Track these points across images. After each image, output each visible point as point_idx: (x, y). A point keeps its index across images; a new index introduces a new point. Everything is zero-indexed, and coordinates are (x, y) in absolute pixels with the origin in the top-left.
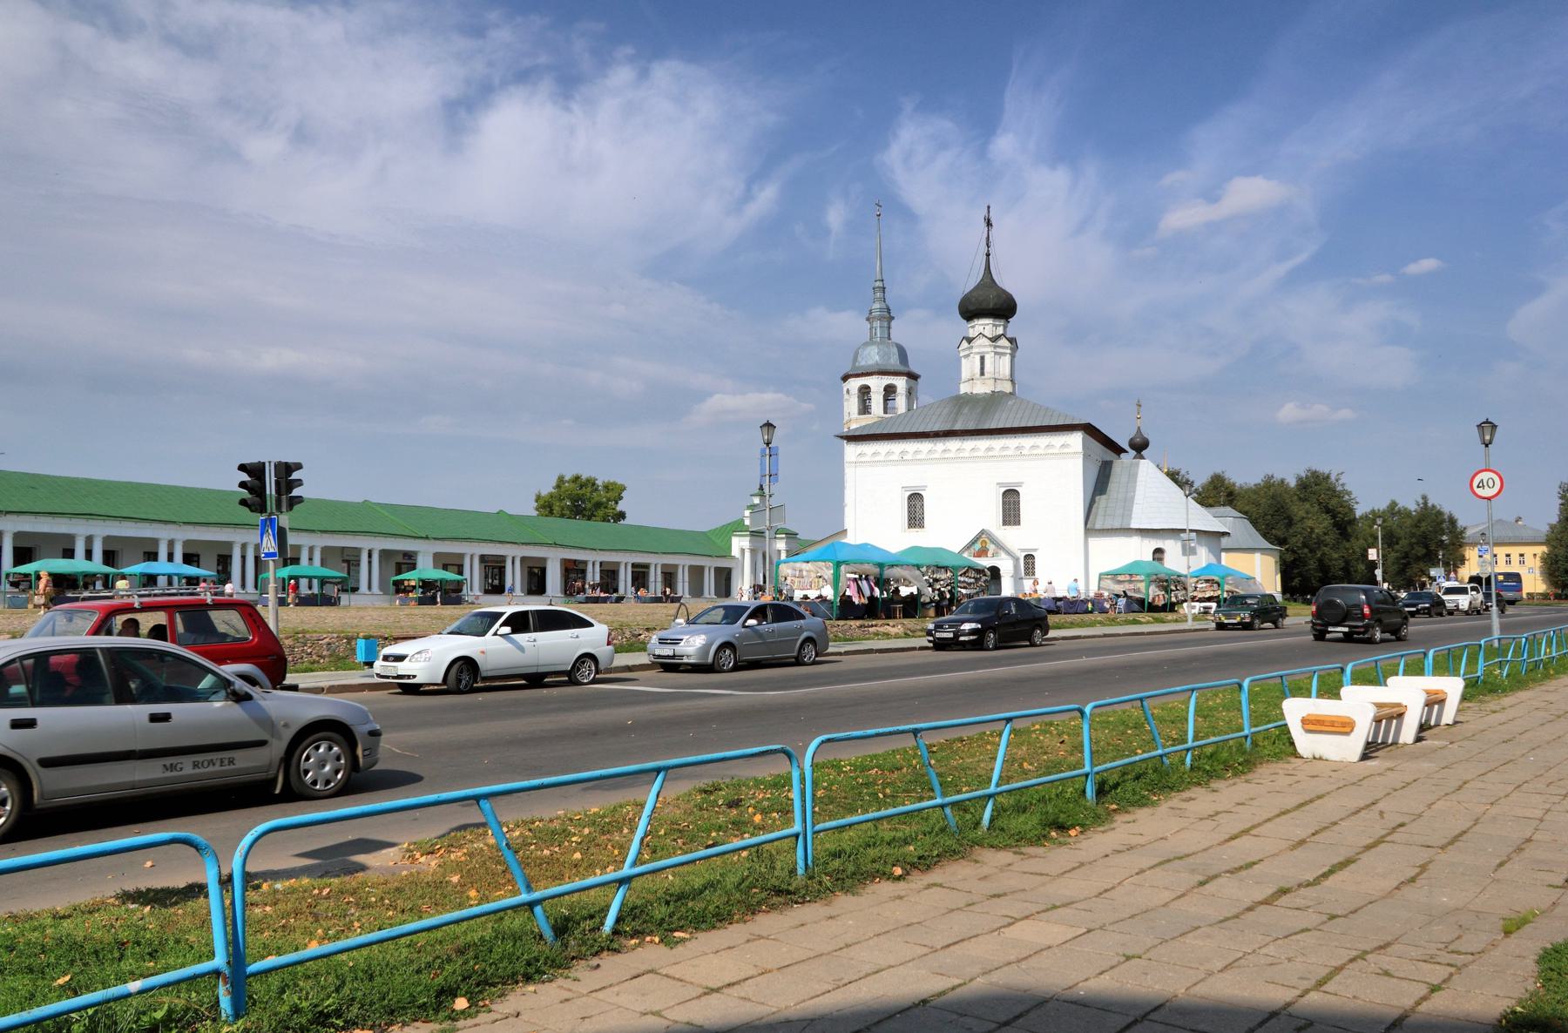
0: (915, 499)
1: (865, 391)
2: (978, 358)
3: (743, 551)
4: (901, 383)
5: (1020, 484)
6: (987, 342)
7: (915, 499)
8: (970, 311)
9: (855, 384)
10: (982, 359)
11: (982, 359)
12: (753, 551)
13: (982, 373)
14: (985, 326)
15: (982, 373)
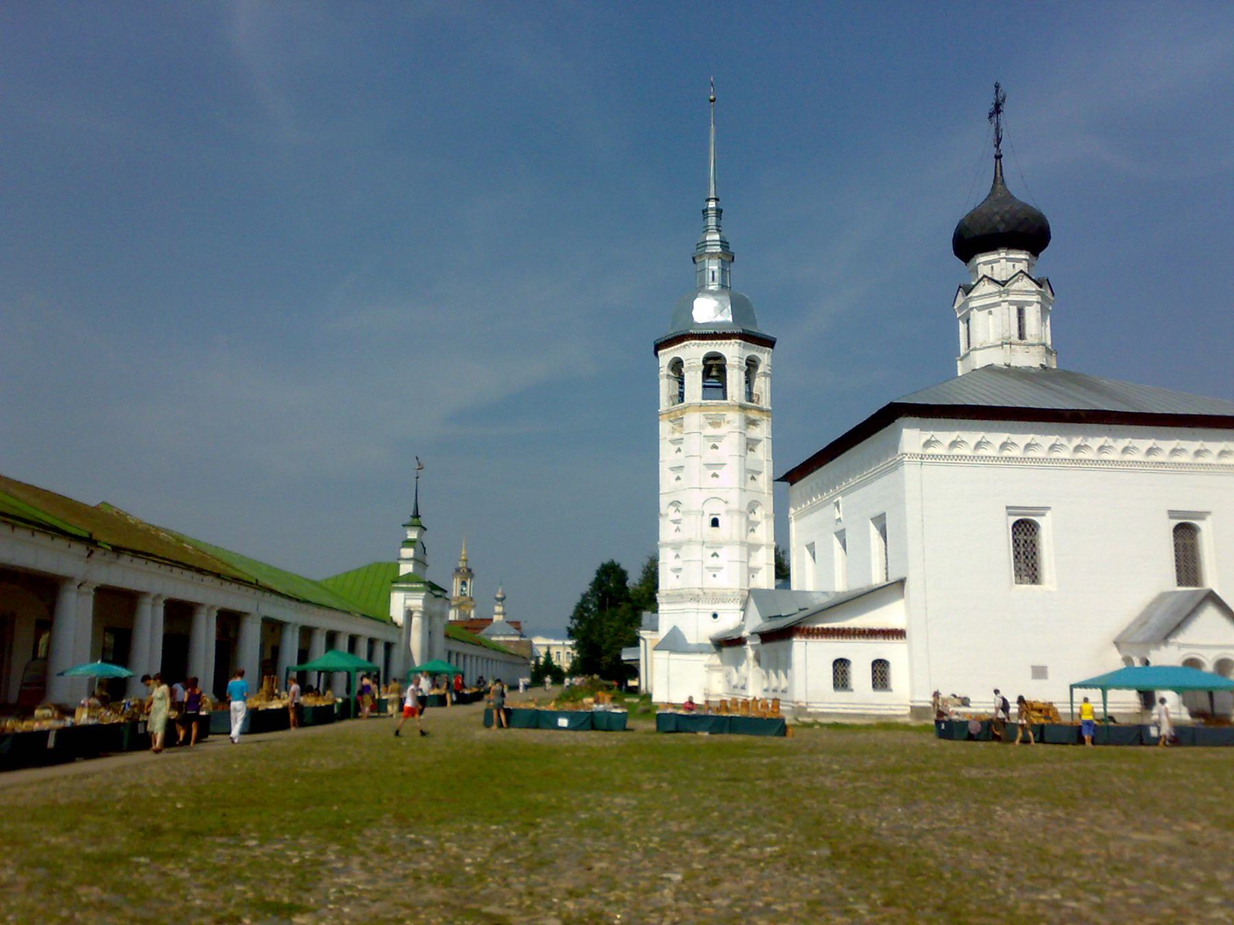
0: (1025, 532)
1: (714, 369)
2: (1014, 309)
3: (409, 614)
4: (764, 357)
5: (1201, 515)
6: (1034, 287)
7: (1025, 532)
8: (971, 242)
9: (693, 354)
10: (1021, 313)
11: (1021, 313)
12: (428, 616)
13: (1022, 336)
14: (1001, 264)
15: (1022, 336)
